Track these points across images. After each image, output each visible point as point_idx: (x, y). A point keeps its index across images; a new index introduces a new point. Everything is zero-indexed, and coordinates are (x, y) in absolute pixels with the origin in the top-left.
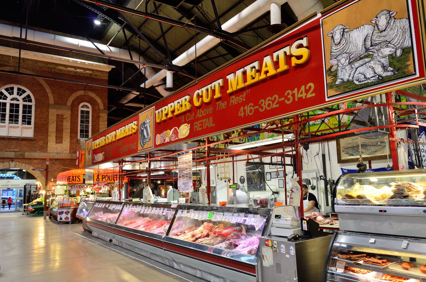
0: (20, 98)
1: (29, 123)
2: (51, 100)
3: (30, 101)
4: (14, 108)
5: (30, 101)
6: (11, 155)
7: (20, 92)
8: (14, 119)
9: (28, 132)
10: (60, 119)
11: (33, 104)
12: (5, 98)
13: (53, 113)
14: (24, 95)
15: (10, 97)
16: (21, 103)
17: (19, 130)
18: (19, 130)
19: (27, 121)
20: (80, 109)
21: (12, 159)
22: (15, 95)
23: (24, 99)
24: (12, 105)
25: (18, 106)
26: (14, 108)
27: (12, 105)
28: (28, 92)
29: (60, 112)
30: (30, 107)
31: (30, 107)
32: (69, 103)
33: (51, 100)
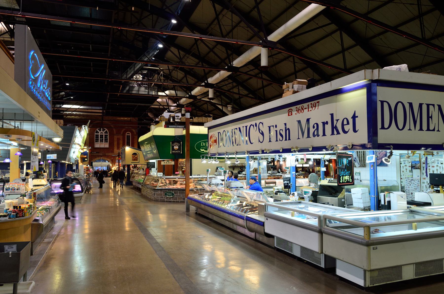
0: (103, 132)
1: (107, 142)
2: (115, 133)
3: (107, 133)
4: (102, 136)
5: (107, 133)
6: (101, 154)
7: (104, 130)
8: (102, 141)
9: (107, 146)
10: (118, 139)
11: (108, 134)
12: (98, 133)
13: (116, 137)
14: (105, 131)
15: (100, 132)
16: (104, 134)
17: (103, 145)
18: (103, 145)
19: (106, 141)
20: (126, 135)
21: (101, 156)
22: (102, 131)
23: (105, 133)
24: (101, 135)
25: (103, 135)
26: (102, 136)
27: (101, 135)
28: (106, 130)
29: (118, 137)
30: (107, 135)
31: (107, 135)
32: (122, 133)
33: (115, 133)
